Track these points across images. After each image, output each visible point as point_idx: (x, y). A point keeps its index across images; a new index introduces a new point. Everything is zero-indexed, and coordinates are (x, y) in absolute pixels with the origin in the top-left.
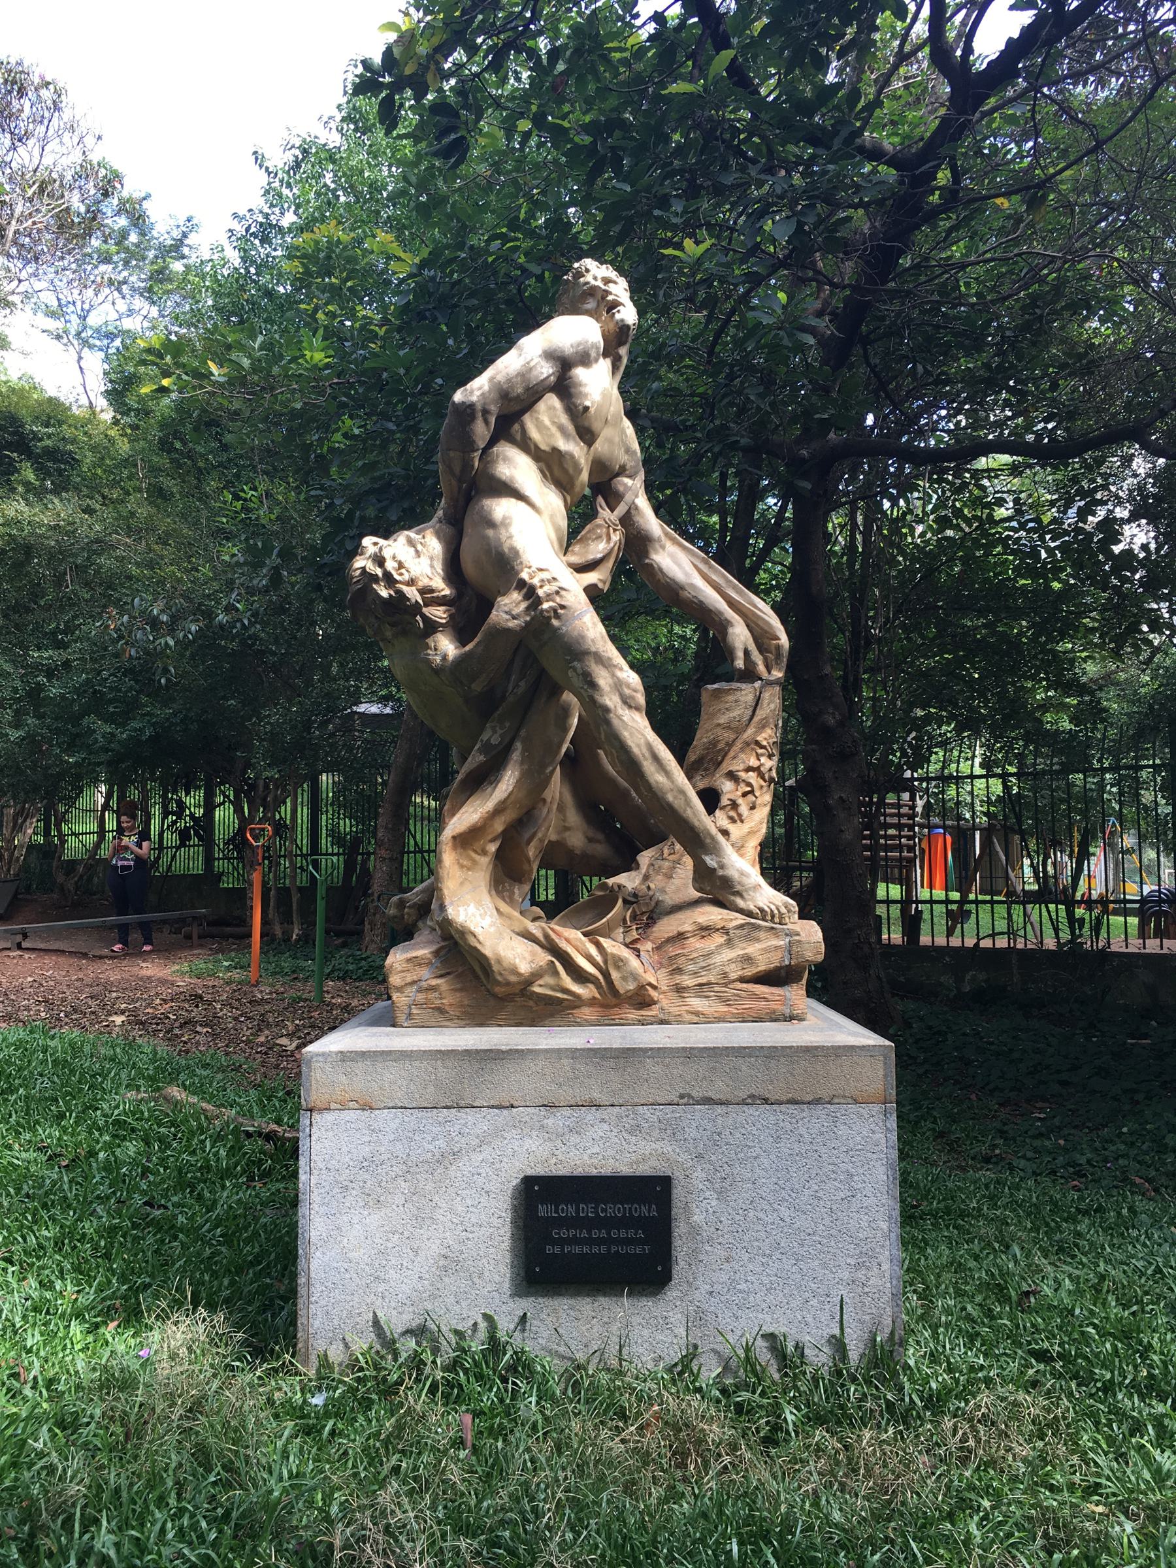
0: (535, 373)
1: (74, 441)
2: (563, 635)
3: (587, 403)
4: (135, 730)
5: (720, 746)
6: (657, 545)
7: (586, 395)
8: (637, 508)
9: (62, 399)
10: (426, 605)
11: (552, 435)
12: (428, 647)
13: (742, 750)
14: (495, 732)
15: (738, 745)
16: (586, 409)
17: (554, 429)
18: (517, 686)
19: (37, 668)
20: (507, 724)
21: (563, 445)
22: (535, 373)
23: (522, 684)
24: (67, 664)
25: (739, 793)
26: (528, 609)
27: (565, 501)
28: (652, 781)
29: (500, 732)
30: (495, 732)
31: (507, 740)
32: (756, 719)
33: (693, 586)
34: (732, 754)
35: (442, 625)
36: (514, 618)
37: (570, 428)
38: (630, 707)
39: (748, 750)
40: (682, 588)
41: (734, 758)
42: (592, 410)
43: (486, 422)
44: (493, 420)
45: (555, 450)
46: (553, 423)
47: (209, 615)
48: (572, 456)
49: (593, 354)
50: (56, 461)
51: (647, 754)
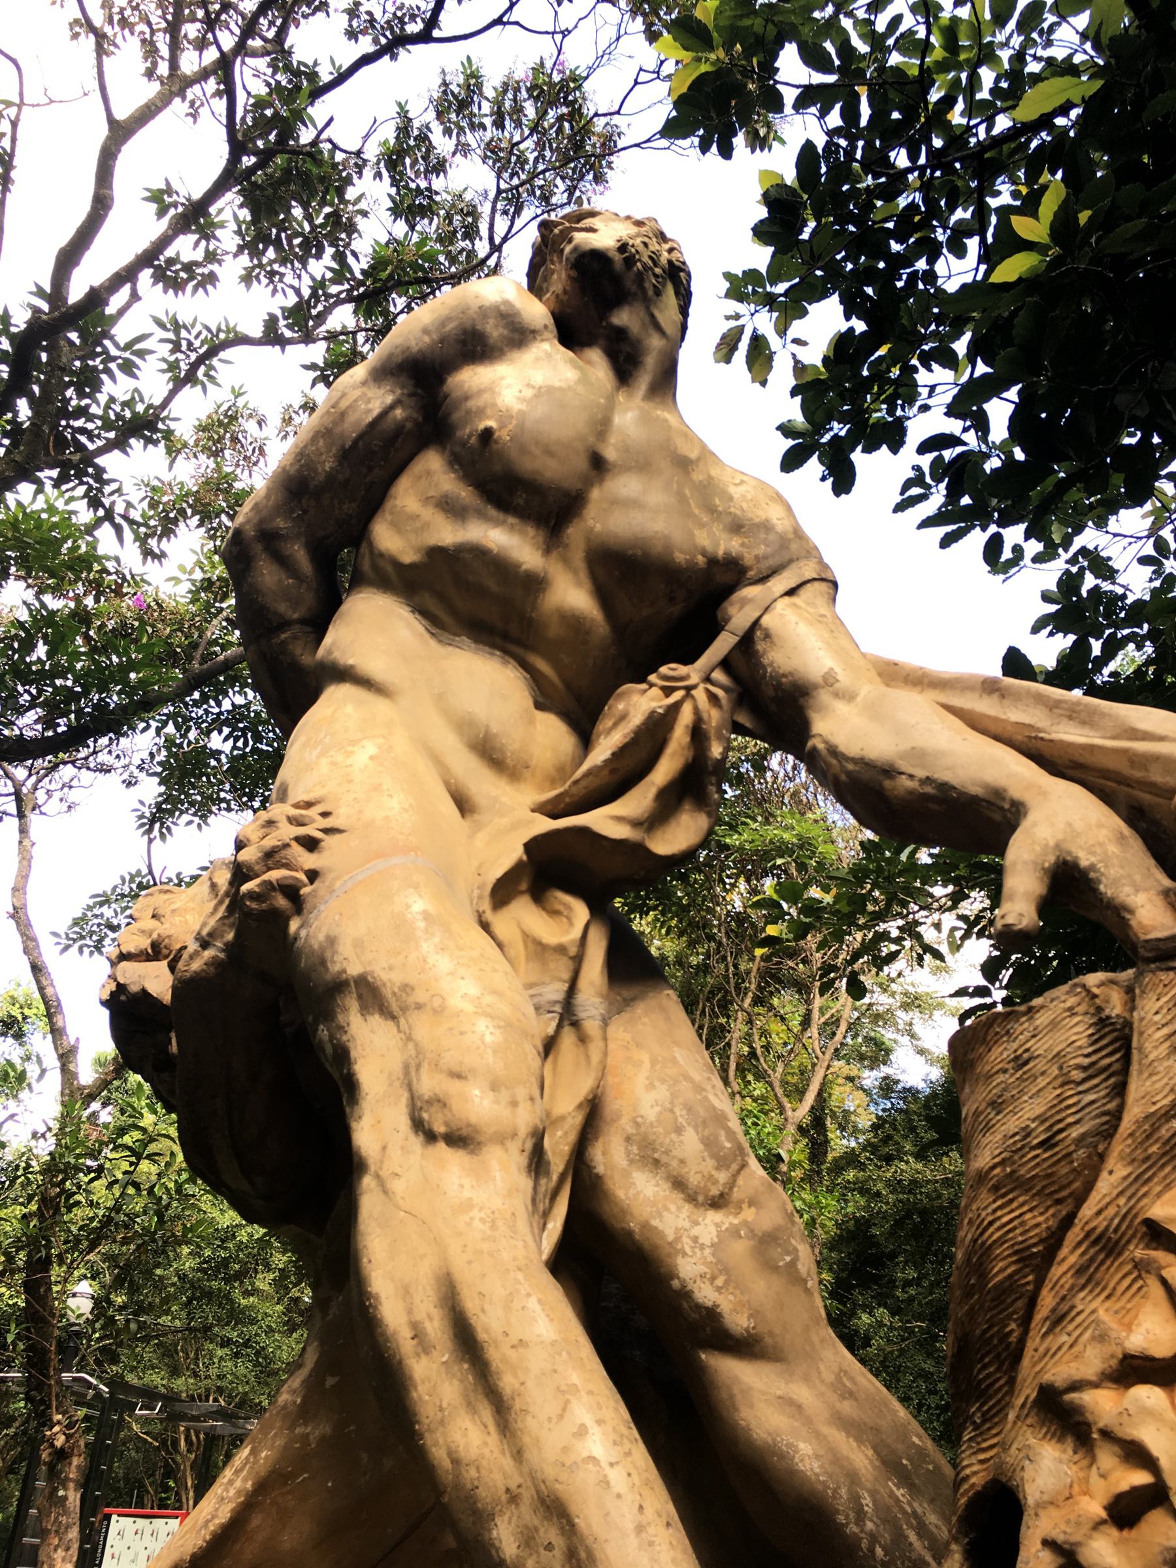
0: (352, 418)
3: (491, 423)
5: (1001, 1269)
6: (824, 696)
7: (481, 413)
8: (767, 636)
11: (426, 526)
13: (1087, 1275)
15: (1069, 1257)
16: (488, 433)
17: (429, 514)
21: (448, 534)
22: (352, 418)
25: (1095, 1508)
27: (525, 665)
28: (439, 1455)
32: (1127, 1123)
33: (918, 754)
34: (1047, 1301)
37: (464, 493)
38: (431, 1137)
39: (1116, 1274)
40: (889, 771)
41: (1058, 1320)
42: (503, 435)
43: (283, 561)
44: (299, 553)
45: (437, 554)
46: (426, 500)
48: (479, 552)
49: (494, 331)
51: (436, 1327)
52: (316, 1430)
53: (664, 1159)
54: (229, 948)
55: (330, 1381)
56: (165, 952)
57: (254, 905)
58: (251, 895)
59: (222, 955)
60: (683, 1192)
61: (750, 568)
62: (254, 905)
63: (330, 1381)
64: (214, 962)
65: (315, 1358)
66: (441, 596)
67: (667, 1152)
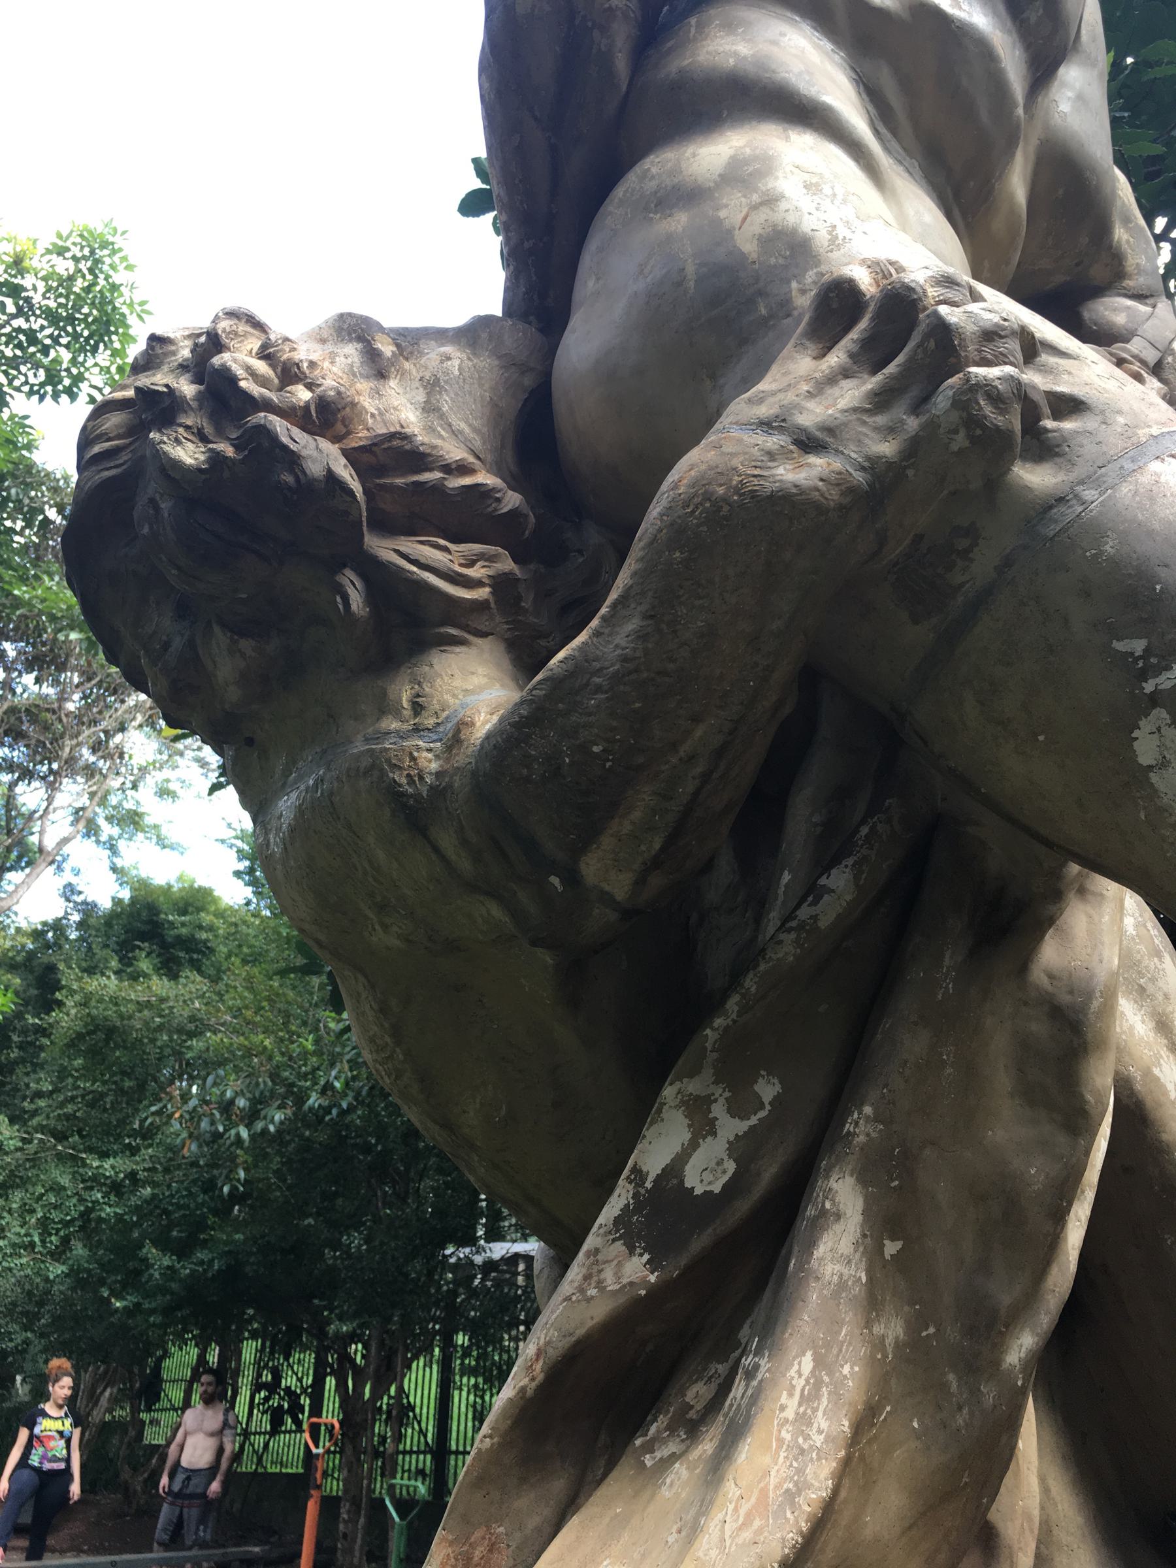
1: (211, 928)
2: (1096, 531)
4: (202, 1263)
9: (216, 893)
10: (386, 526)
12: (385, 707)
14: (703, 1128)
18: (812, 891)
19: (95, 1181)
20: (767, 1090)
23: (839, 880)
24: (132, 1175)
26: (881, 401)
29: (730, 1127)
30: (703, 1128)
31: (769, 1171)
35: (455, 612)
36: (808, 443)
47: (300, 1099)
50: (188, 951)
52: (892, 1329)
53: (1151, 989)
54: (872, 465)
55: (891, 1248)
56: (340, 428)
57: (988, 409)
58: (987, 389)
59: (859, 477)
60: (1166, 1037)
61: (1130, 277)
62: (988, 409)
63: (891, 1248)
64: (839, 481)
65: (860, 1204)
66: (906, 84)
67: (1153, 980)
